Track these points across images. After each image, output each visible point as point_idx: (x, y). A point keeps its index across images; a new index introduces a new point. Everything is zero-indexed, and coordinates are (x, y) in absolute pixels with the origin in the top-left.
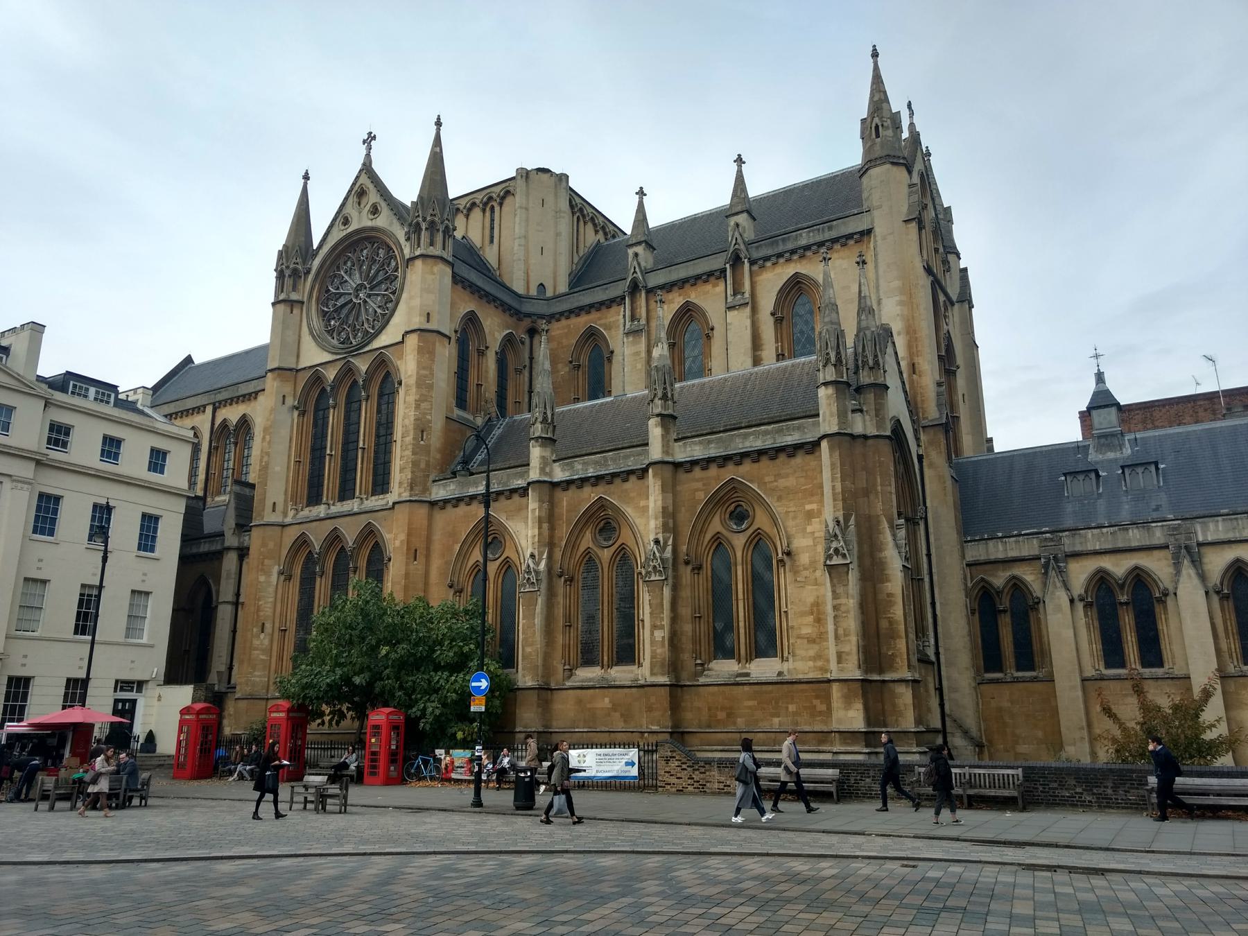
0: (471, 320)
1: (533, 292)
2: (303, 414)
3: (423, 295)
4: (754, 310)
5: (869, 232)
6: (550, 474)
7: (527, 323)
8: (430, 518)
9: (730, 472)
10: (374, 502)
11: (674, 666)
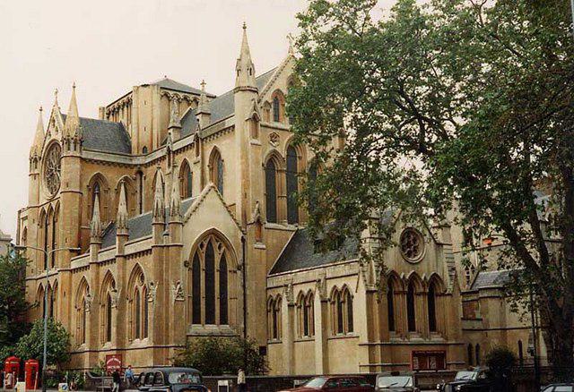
0: (98, 181)
1: (141, 152)
2: (41, 227)
3: (69, 171)
4: (203, 163)
5: (233, 126)
6: (97, 259)
7: (135, 169)
8: (71, 277)
9: (138, 260)
10: (53, 271)
11: (120, 342)
